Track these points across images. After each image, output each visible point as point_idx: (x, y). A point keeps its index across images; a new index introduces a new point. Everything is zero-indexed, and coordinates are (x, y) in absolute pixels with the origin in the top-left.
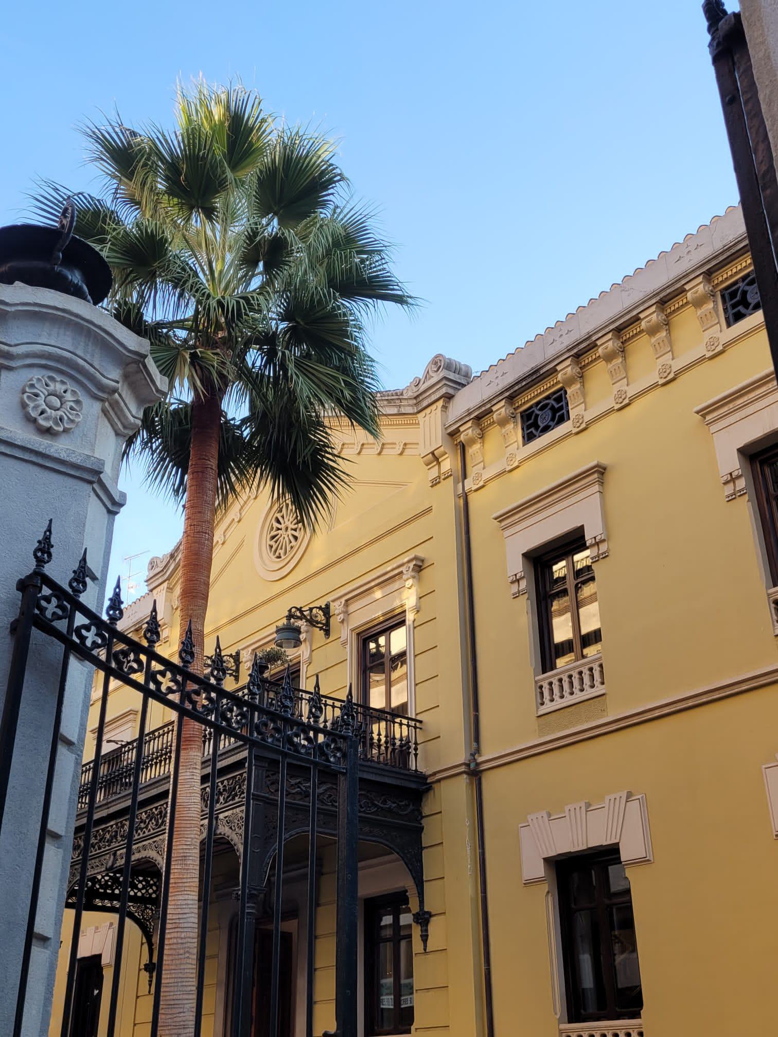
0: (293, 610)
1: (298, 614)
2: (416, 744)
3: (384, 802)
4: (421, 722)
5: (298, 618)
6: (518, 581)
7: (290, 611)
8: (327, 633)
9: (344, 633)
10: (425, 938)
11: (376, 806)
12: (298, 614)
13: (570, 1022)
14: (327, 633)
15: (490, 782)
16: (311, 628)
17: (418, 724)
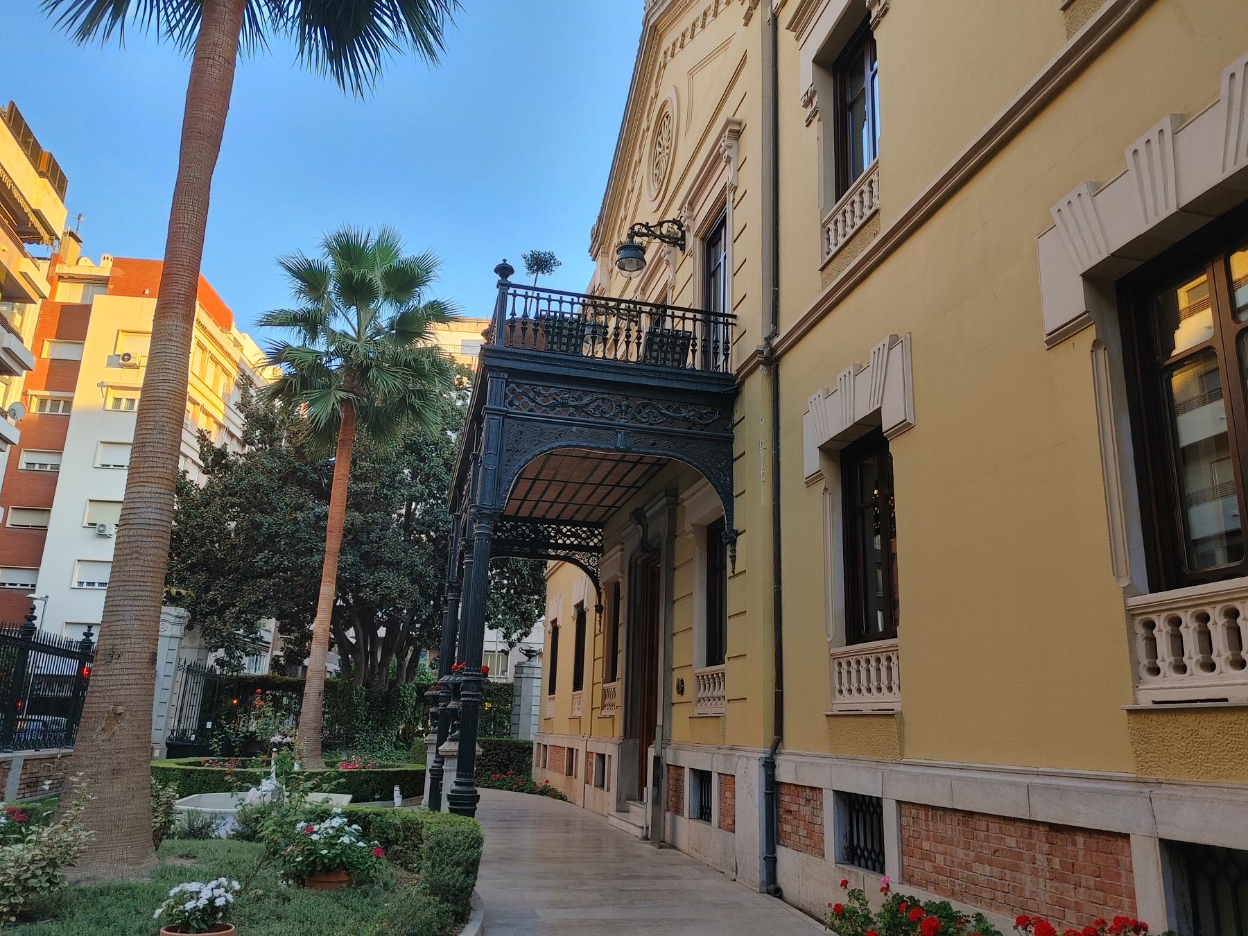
0: (637, 228)
1: (644, 231)
2: (727, 342)
3: (678, 411)
4: (735, 317)
5: (643, 235)
6: (810, 100)
7: (632, 228)
8: (683, 248)
9: (692, 242)
10: (733, 558)
11: (664, 415)
12: (644, 231)
13: (849, 642)
14: (683, 248)
15: (791, 366)
16: (672, 249)
17: (730, 320)
